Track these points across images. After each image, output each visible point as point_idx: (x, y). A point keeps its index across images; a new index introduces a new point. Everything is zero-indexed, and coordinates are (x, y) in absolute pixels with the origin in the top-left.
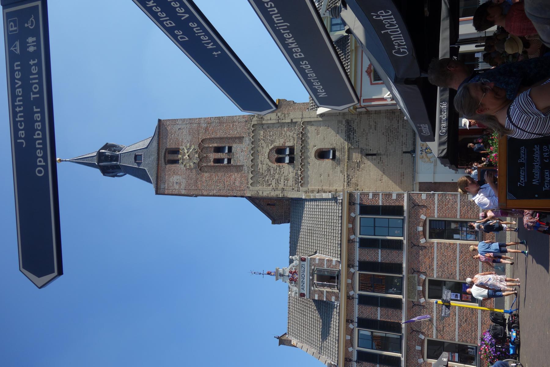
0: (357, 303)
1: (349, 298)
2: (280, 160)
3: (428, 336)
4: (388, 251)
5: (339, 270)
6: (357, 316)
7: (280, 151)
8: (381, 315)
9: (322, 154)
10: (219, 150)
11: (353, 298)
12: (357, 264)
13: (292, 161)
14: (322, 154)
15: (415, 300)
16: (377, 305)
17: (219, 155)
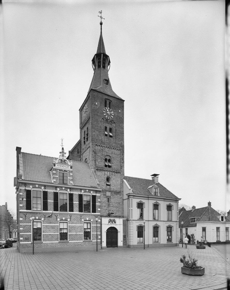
0: (54, 191)
1: (56, 187)
2: (106, 160)
3: (43, 222)
4: (78, 206)
5: (68, 184)
6: (48, 191)
7: (109, 161)
8: (50, 202)
9: (108, 179)
10: (111, 130)
11: (56, 190)
12: (72, 193)
13: (106, 166)
14: (108, 179)
15: (58, 217)
16: (54, 200)
17: (108, 129)
